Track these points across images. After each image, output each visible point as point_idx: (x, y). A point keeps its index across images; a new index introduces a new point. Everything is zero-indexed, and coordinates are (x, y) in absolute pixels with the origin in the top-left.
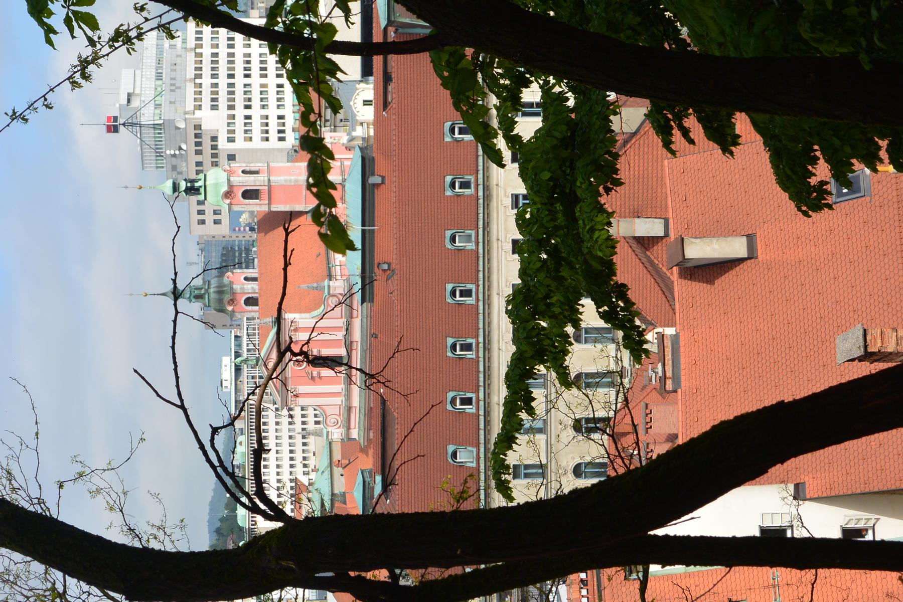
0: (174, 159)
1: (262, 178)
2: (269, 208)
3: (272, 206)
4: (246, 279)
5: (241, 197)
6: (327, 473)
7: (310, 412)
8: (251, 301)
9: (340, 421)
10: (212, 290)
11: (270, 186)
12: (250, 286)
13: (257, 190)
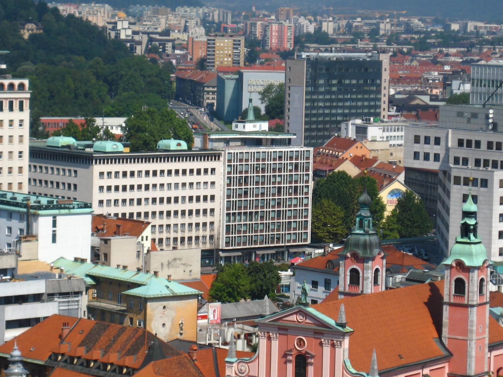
0: (484, 117)
1: (475, 299)
2: (446, 303)
3: (448, 307)
4: (377, 270)
5: (458, 276)
6: (166, 292)
7: (208, 219)
8: (355, 274)
9: (243, 375)
10: (367, 238)
11: (467, 306)
12: (370, 275)
13: (464, 293)
